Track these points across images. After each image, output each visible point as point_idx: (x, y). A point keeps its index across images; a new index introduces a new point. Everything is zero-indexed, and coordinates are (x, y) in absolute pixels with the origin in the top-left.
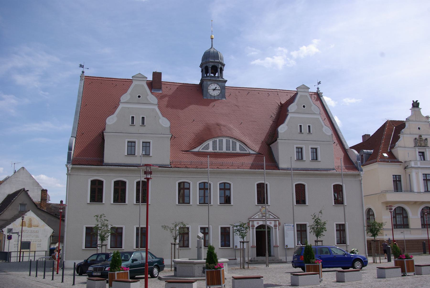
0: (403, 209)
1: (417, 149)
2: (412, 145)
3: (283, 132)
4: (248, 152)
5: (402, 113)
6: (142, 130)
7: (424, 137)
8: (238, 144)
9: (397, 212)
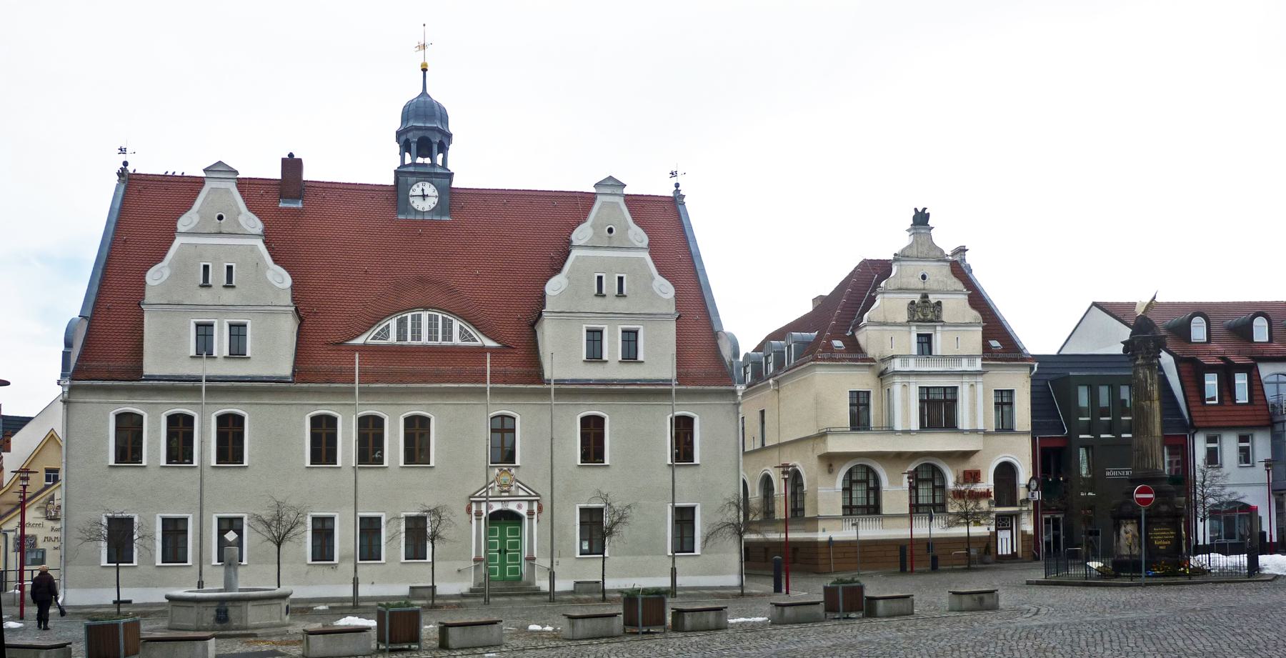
0: (869, 470)
1: (914, 328)
2: (903, 316)
4: (479, 343)
5: (889, 240)
6: (228, 297)
7: (933, 299)
8: (457, 324)
9: (854, 478)
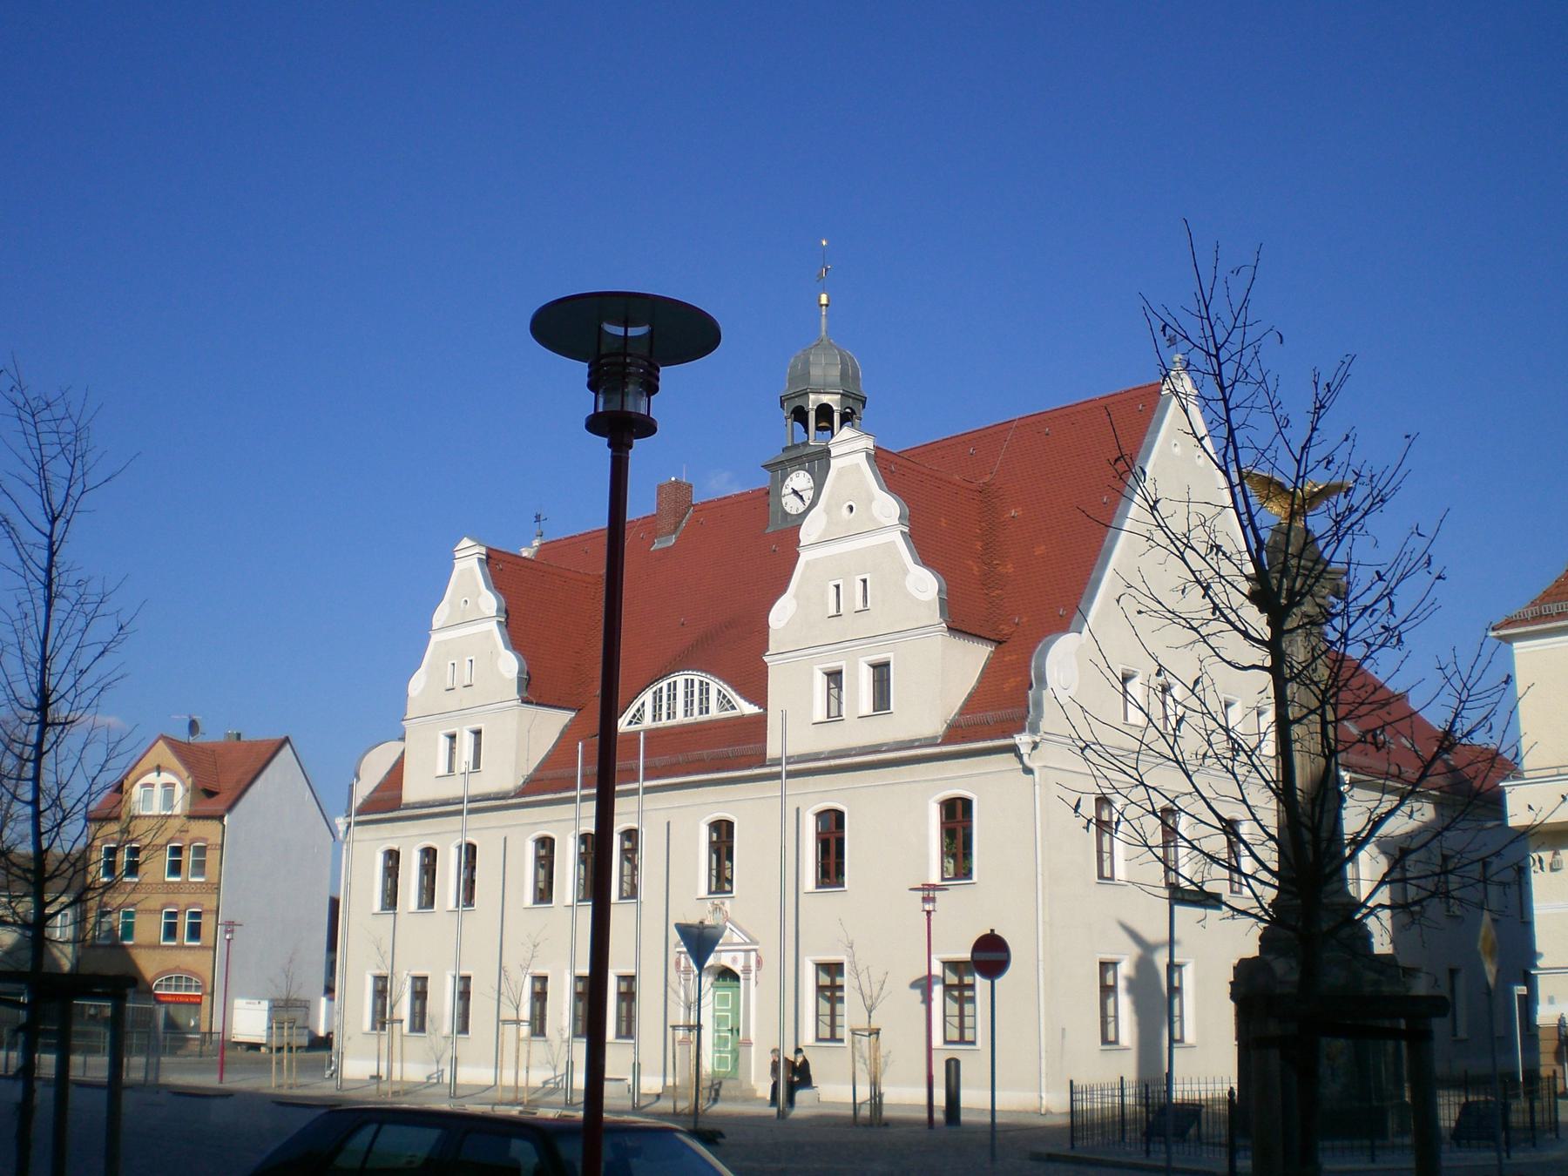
3: (782, 624)
